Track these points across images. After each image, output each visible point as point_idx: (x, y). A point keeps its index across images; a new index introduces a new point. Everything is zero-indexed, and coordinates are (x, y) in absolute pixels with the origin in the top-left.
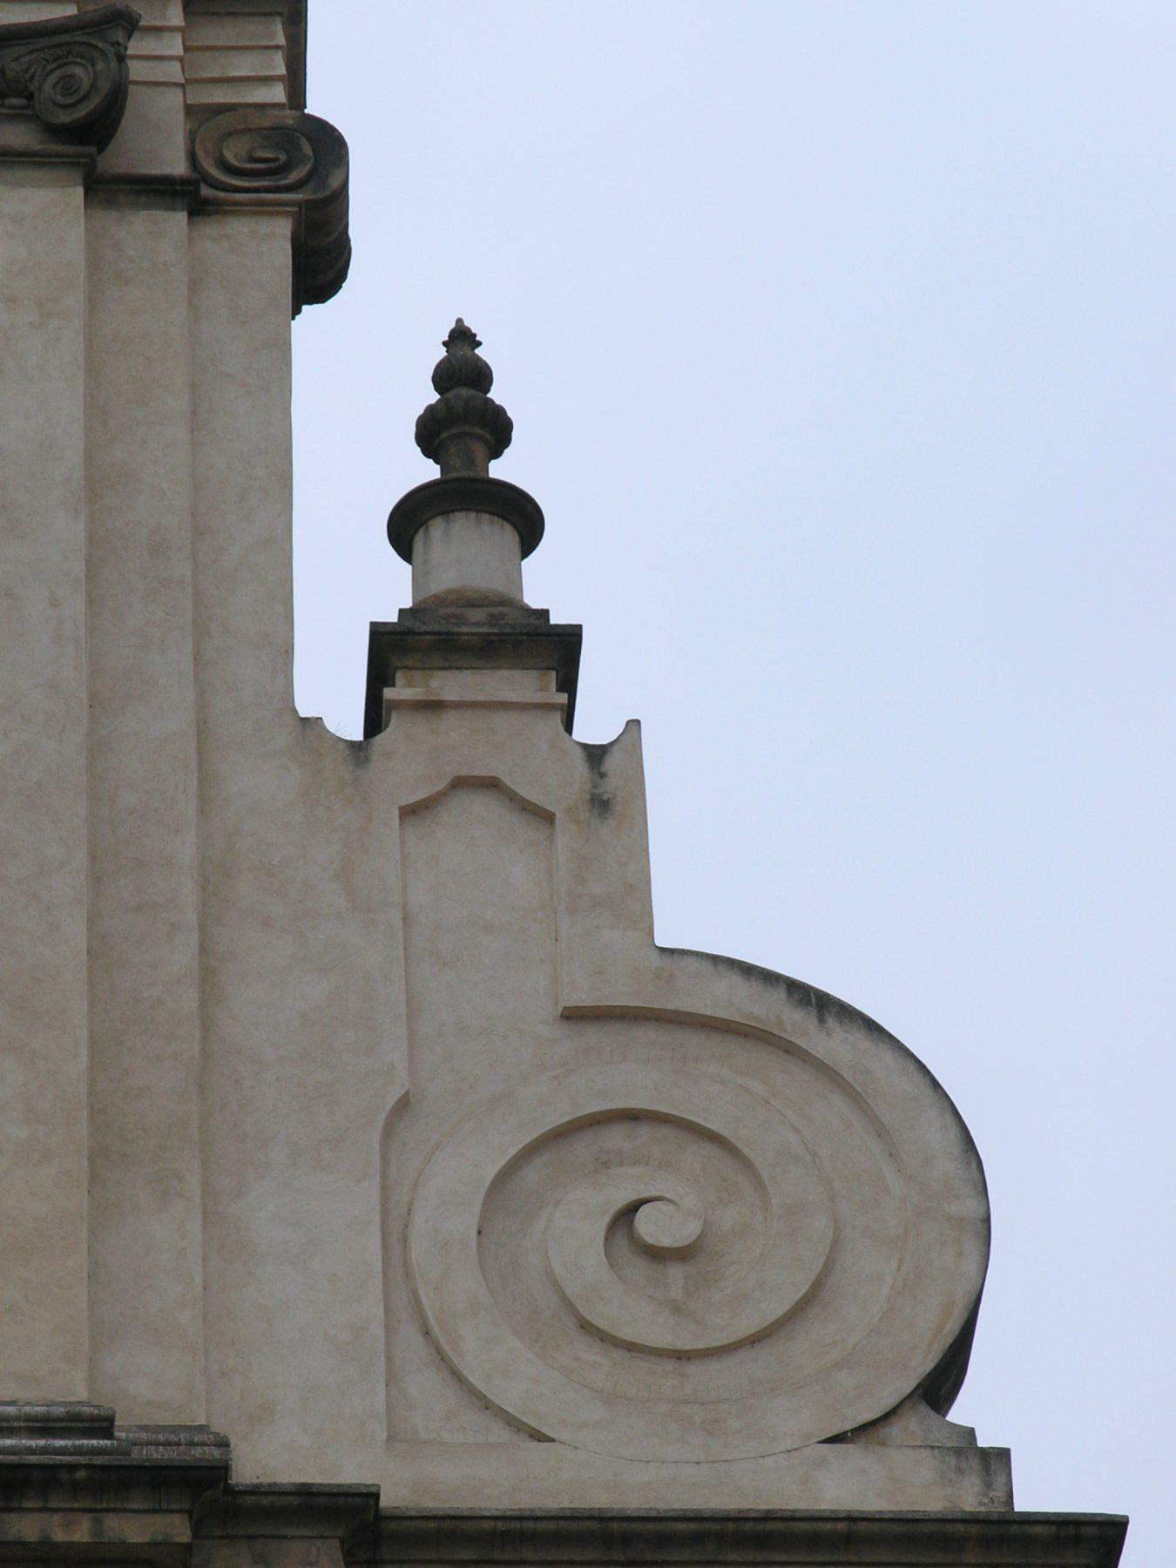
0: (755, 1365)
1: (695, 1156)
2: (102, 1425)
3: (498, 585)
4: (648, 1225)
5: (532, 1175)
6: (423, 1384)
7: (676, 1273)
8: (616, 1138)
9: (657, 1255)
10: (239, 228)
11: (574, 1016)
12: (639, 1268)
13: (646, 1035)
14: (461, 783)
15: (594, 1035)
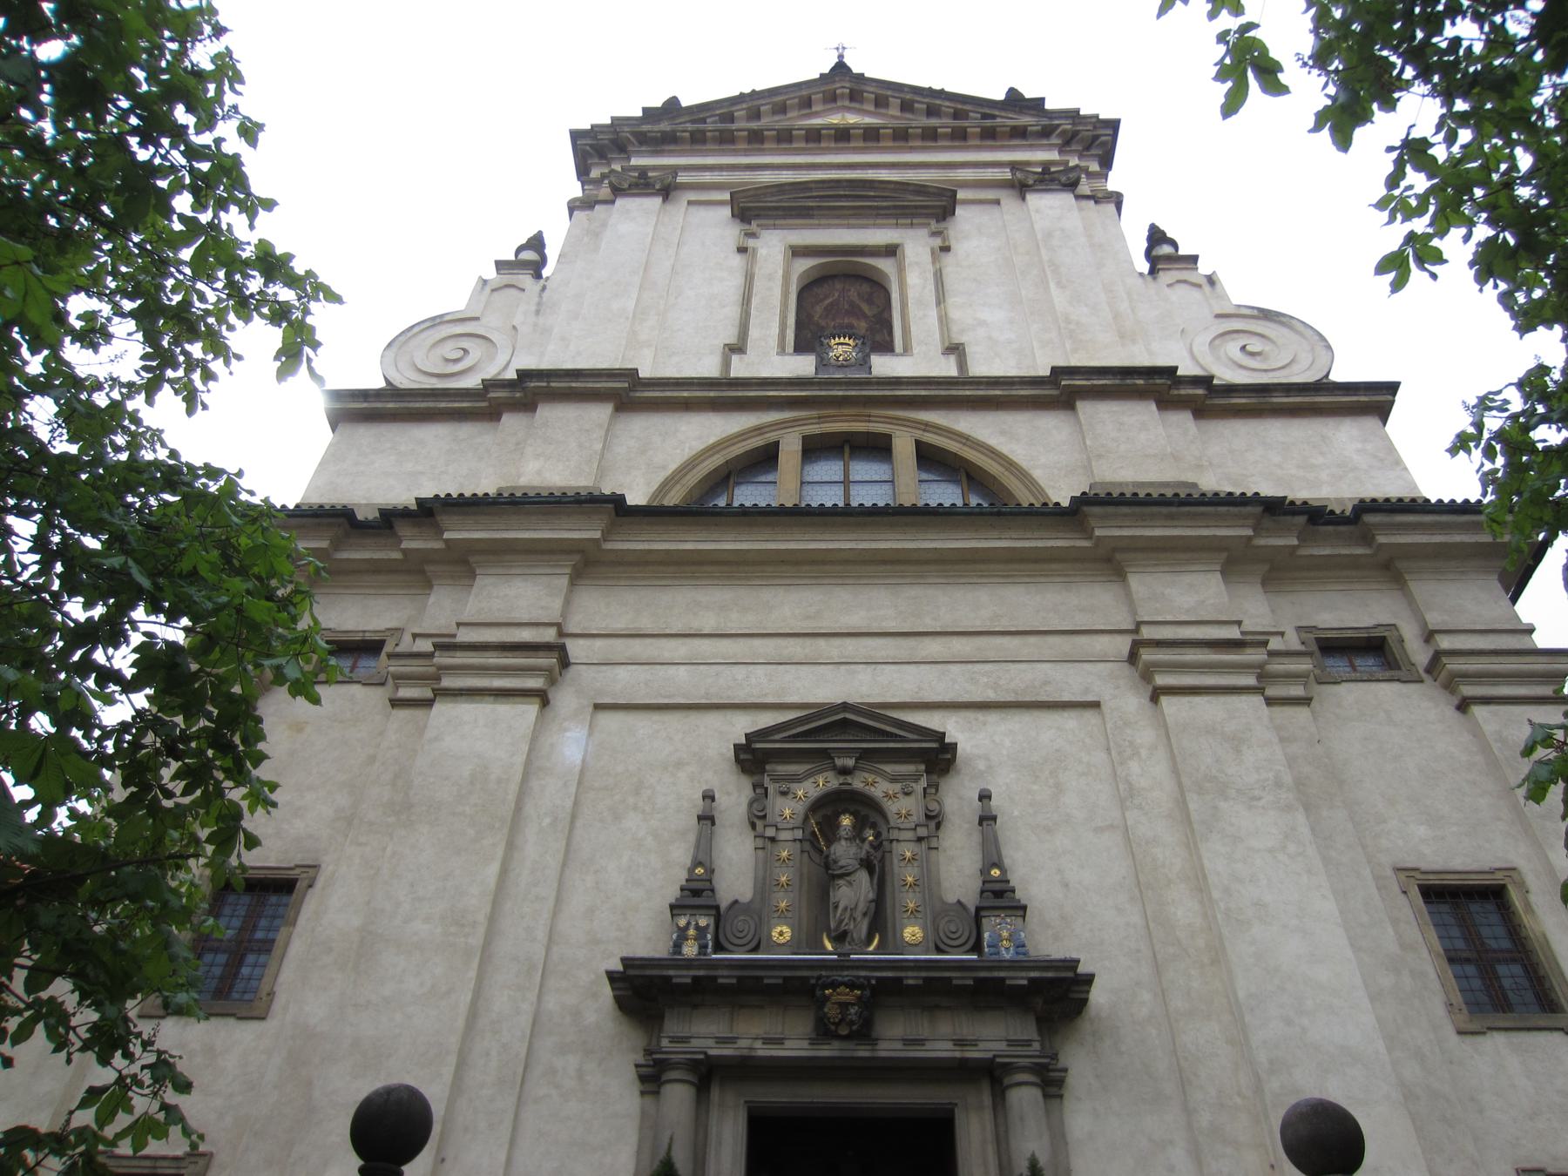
11: (1218, 316)
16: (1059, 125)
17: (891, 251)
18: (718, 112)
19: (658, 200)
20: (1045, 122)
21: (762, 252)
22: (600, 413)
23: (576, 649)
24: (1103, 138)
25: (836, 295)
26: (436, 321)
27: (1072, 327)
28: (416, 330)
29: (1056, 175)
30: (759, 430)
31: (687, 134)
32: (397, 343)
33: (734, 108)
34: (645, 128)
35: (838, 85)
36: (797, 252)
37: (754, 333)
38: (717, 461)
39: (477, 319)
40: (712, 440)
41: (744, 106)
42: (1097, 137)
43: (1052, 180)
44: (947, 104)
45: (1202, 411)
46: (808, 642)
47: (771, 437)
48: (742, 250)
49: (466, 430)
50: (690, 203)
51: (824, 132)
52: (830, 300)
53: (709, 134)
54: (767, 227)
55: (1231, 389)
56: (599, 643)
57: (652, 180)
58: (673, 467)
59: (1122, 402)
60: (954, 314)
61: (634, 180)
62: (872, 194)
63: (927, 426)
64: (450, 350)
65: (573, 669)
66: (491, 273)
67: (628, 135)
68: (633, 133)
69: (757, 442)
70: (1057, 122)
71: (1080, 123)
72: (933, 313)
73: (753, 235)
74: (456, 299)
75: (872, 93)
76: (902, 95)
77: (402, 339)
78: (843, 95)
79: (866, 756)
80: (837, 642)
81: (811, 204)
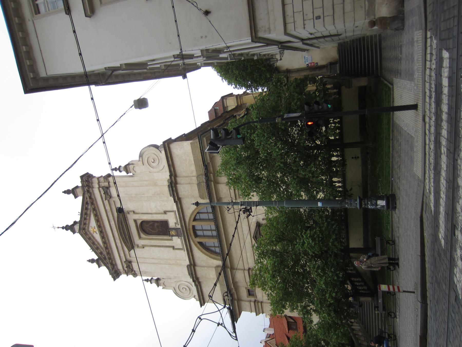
0: (158, 156)
1: (149, 159)
2: (169, 186)
3: (123, 168)
4: (153, 161)
5: (151, 166)
6: (163, 171)
7: (155, 160)
8: (149, 163)
9: (154, 161)
10: (109, 180)
11: (143, 165)
12: (155, 162)
13: (143, 161)
14: (133, 170)
15: (144, 163)
16: (87, 190)
17: (135, 221)
18: (100, 256)
19: (133, 263)
20: (86, 193)
21: (143, 244)
22: (198, 269)
23: (247, 267)
24: (86, 179)
25: (148, 228)
26: (176, 293)
27: (156, 194)
28: (179, 296)
29: (105, 191)
30: (196, 245)
31: (110, 261)
32: (183, 298)
33: (98, 253)
34: (111, 268)
35: (82, 233)
36: (140, 237)
37: (168, 245)
38: (204, 250)
39: (174, 288)
40: (200, 252)
41: (97, 251)
42: (86, 180)
43: (107, 192)
44: (84, 211)
45: (176, 176)
46: (240, 239)
47: (196, 243)
48: (143, 248)
49: (203, 285)
50: (130, 257)
51: (102, 236)
52: (150, 230)
53: (109, 257)
54: (134, 243)
55: (170, 171)
56: (245, 265)
57: (127, 266)
58: (207, 257)
59: (178, 190)
60: (154, 211)
61: (128, 268)
62: (121, 226)
63: (190, 220)
64: (182, 290)
65: (250, 267)
66: (161, 287)
67: (114, 271)
68: (113, 270)
69: (198, 245)
70: (86, 190)
71: (84, 185)
72: (155, 215)
73: (138, 246)
74: (170, 292)
75: (83, 226)
76: (83, 220)
77: (182, 298)
78: (85, 231)
79: (260, 234)
80: (240, 236)
81: (128, 237)
